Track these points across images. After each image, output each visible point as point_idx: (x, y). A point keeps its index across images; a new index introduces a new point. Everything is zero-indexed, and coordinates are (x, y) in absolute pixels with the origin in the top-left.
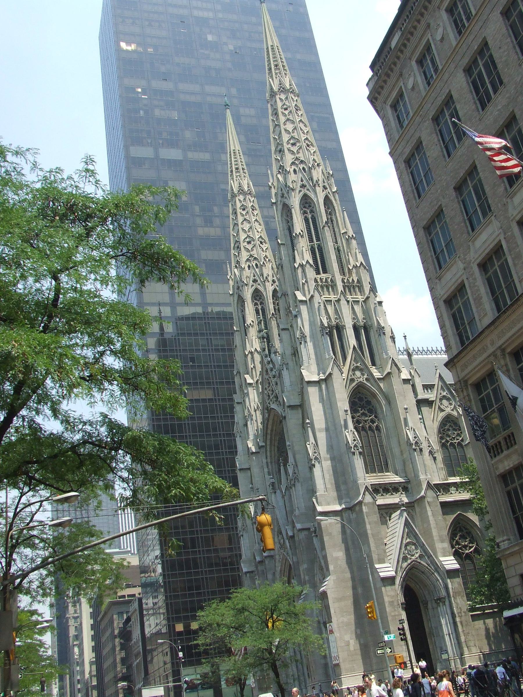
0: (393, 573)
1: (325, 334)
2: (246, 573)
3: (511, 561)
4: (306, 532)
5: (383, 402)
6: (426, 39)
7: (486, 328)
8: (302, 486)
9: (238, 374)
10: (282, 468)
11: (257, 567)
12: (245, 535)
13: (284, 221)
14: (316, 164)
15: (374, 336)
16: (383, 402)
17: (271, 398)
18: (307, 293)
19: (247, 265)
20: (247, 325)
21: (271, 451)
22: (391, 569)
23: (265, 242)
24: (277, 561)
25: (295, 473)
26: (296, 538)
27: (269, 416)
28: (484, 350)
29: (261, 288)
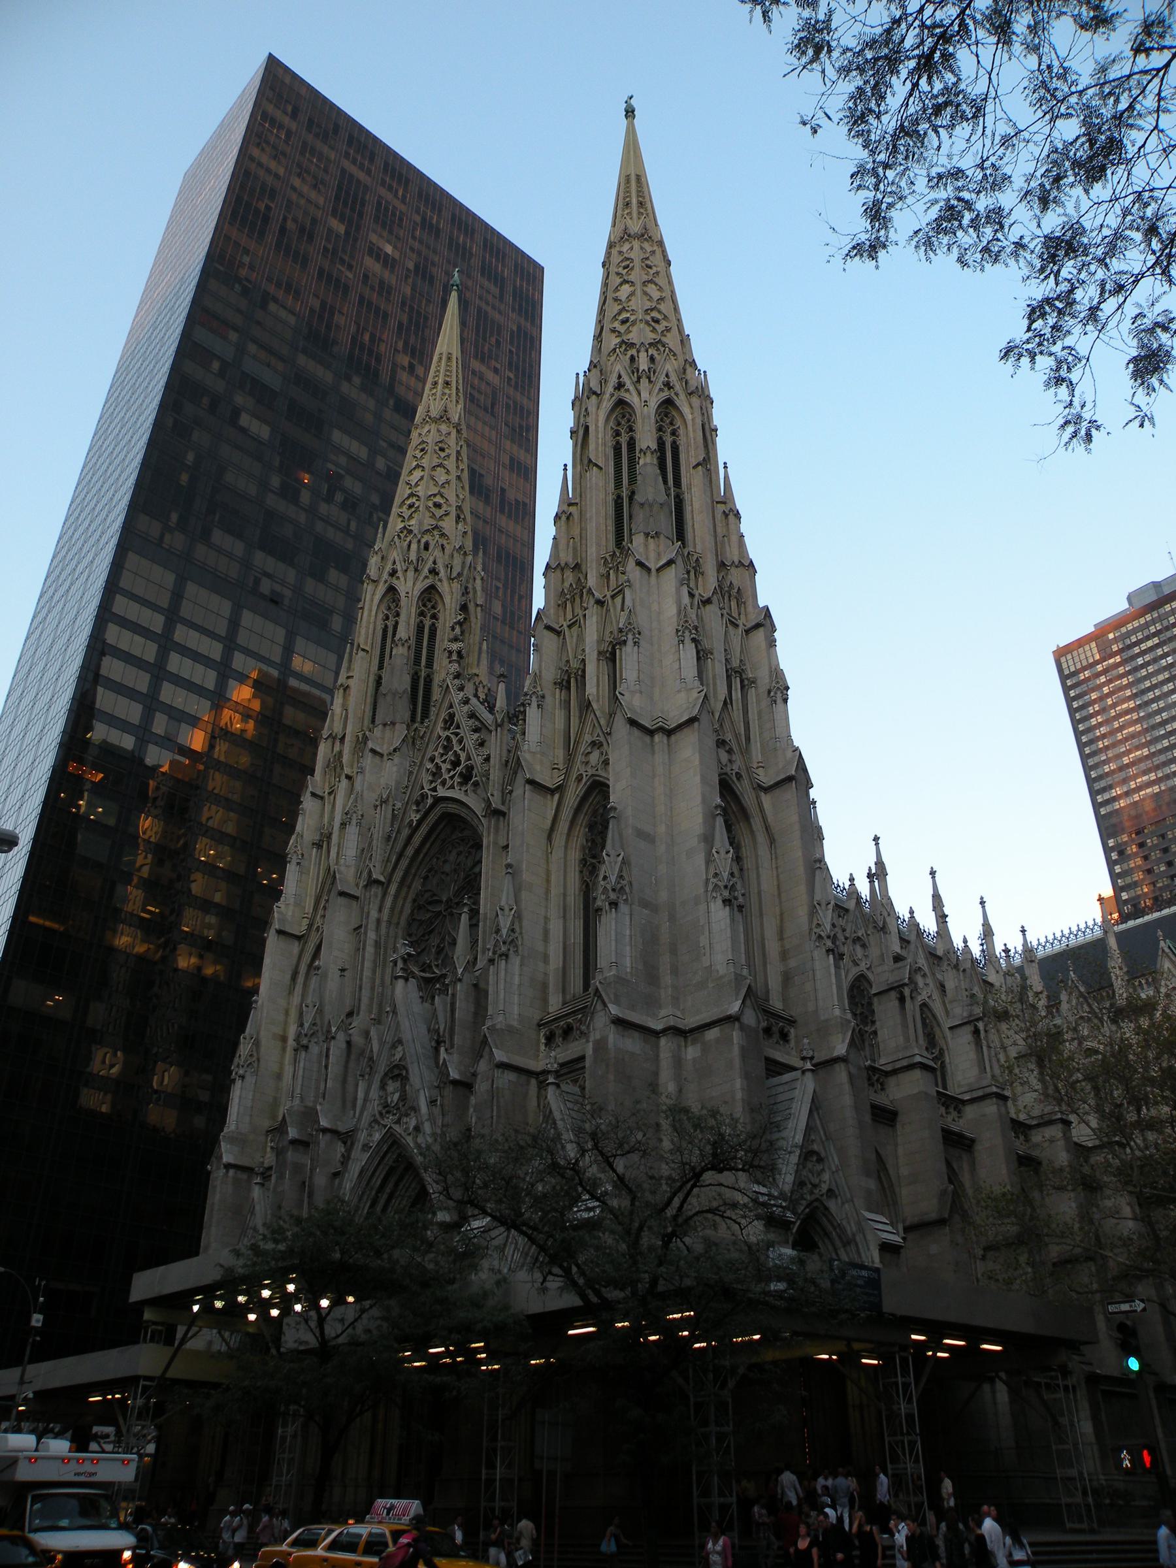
1: (687, 640)
2: (228, 1166)
4: (511, 1076)
5: (761, 838)
9: (330, 740)
12: (250, 1079)
15: (758, 702)
16: (761, 838)
17: (446, 776)
18: (652, 555)
20: (400, 639)
21: (396, 897)
23: (464, 519)
24: (358, 1146)
25: (513, 930)
26: (481, 1087)
29: (444, 587)
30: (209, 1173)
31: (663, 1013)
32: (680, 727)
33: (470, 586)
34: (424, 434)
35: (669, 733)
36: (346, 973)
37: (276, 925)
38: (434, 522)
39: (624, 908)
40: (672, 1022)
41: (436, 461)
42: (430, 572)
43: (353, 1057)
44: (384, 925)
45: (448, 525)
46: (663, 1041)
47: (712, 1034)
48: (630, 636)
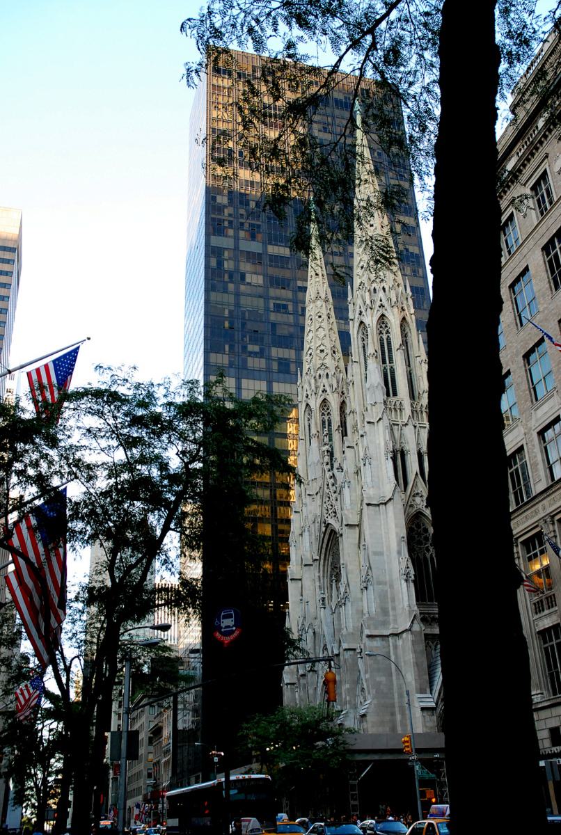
0: (433, 705)
2: (287, 684)
3: (543, 714)
4: (351, 653)
6: (510, 212)
7: (538, 494)
8: (352, 605)
10: (334, 585)
11: (299, 680)
13: (360, 339)
14: (397, 284)
17: (330, 512)
19: (318, 374)
21: (324, 565)
22: (432, 700)
24: (320, 677)
26: (341, 657)
27: (326, 530)
28: (536, 512)
30: (282, 687)
31: (391, 626)
32: (388, 501)
33: (344, 390)
34: (311, 310)
35: (385, 504)
36: (309, 603)
37: (290, 578)
38: (321, 362)
39: (370, 588)
40: (391, 633)
41: (318, 325)
42: (323, 392)
43: (317, 638)
44: (321, 578)
45: (329, 361)
46: (390, 639)
47: (404, 635)
48: (367, 461)
